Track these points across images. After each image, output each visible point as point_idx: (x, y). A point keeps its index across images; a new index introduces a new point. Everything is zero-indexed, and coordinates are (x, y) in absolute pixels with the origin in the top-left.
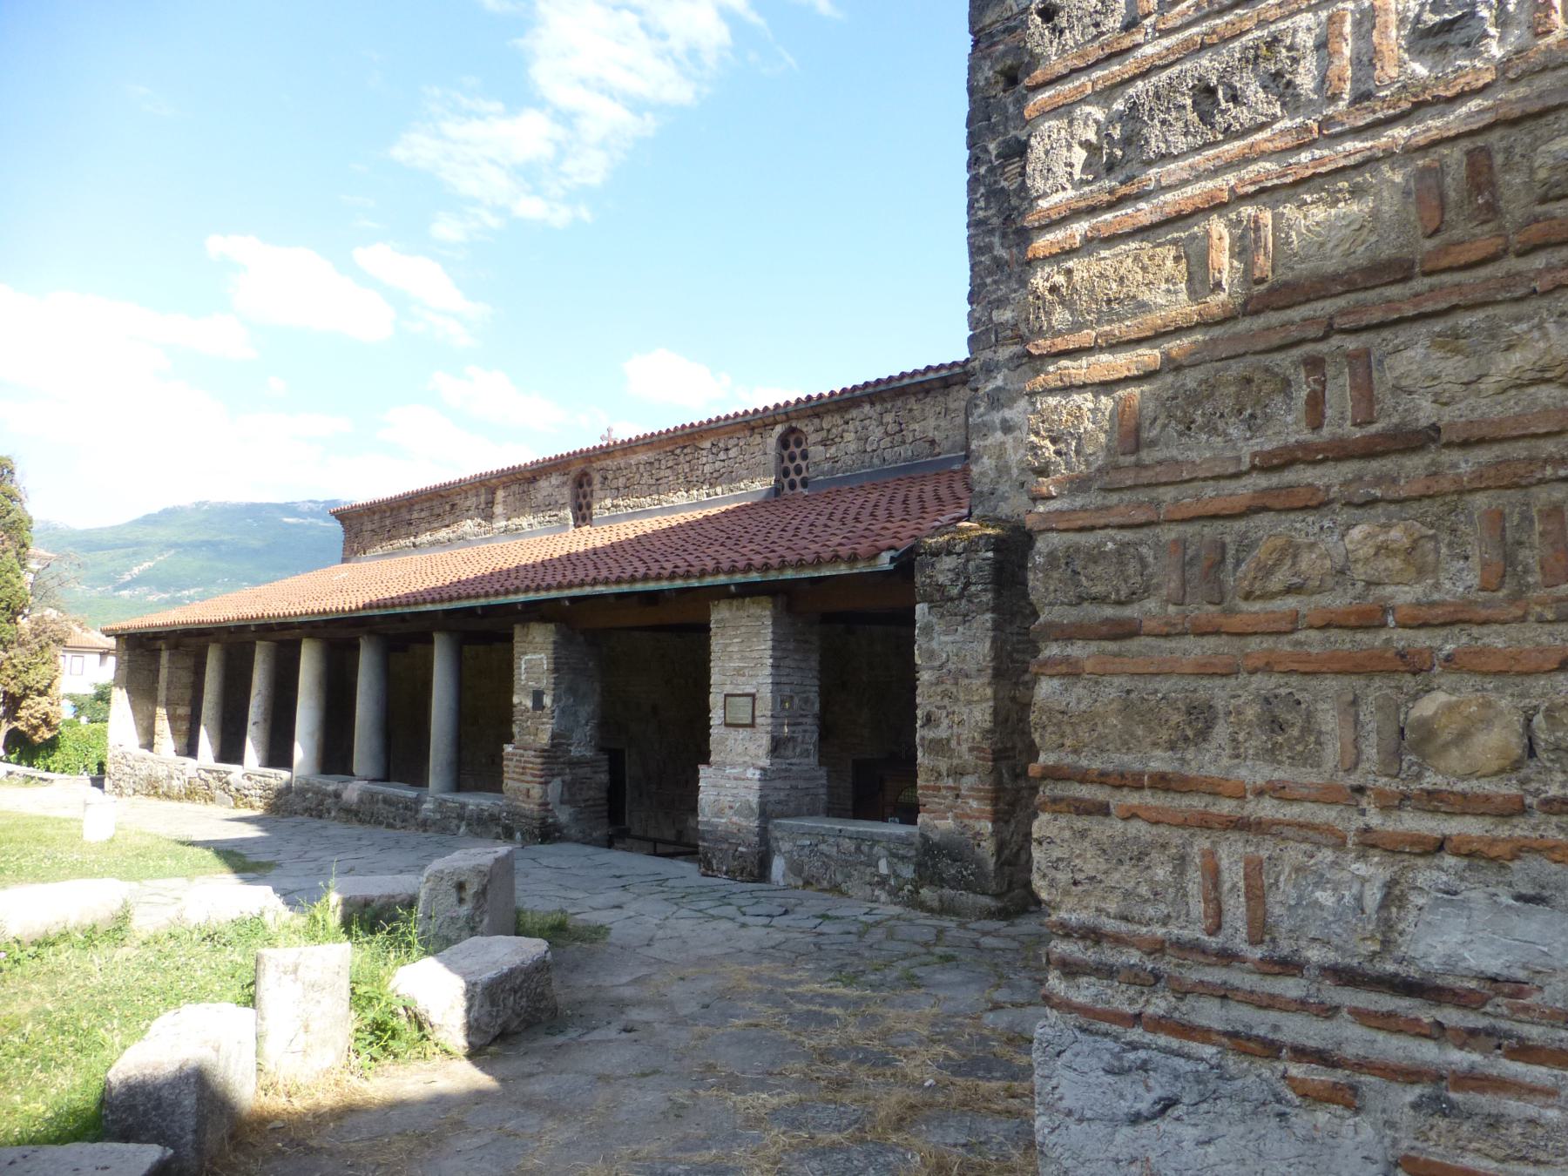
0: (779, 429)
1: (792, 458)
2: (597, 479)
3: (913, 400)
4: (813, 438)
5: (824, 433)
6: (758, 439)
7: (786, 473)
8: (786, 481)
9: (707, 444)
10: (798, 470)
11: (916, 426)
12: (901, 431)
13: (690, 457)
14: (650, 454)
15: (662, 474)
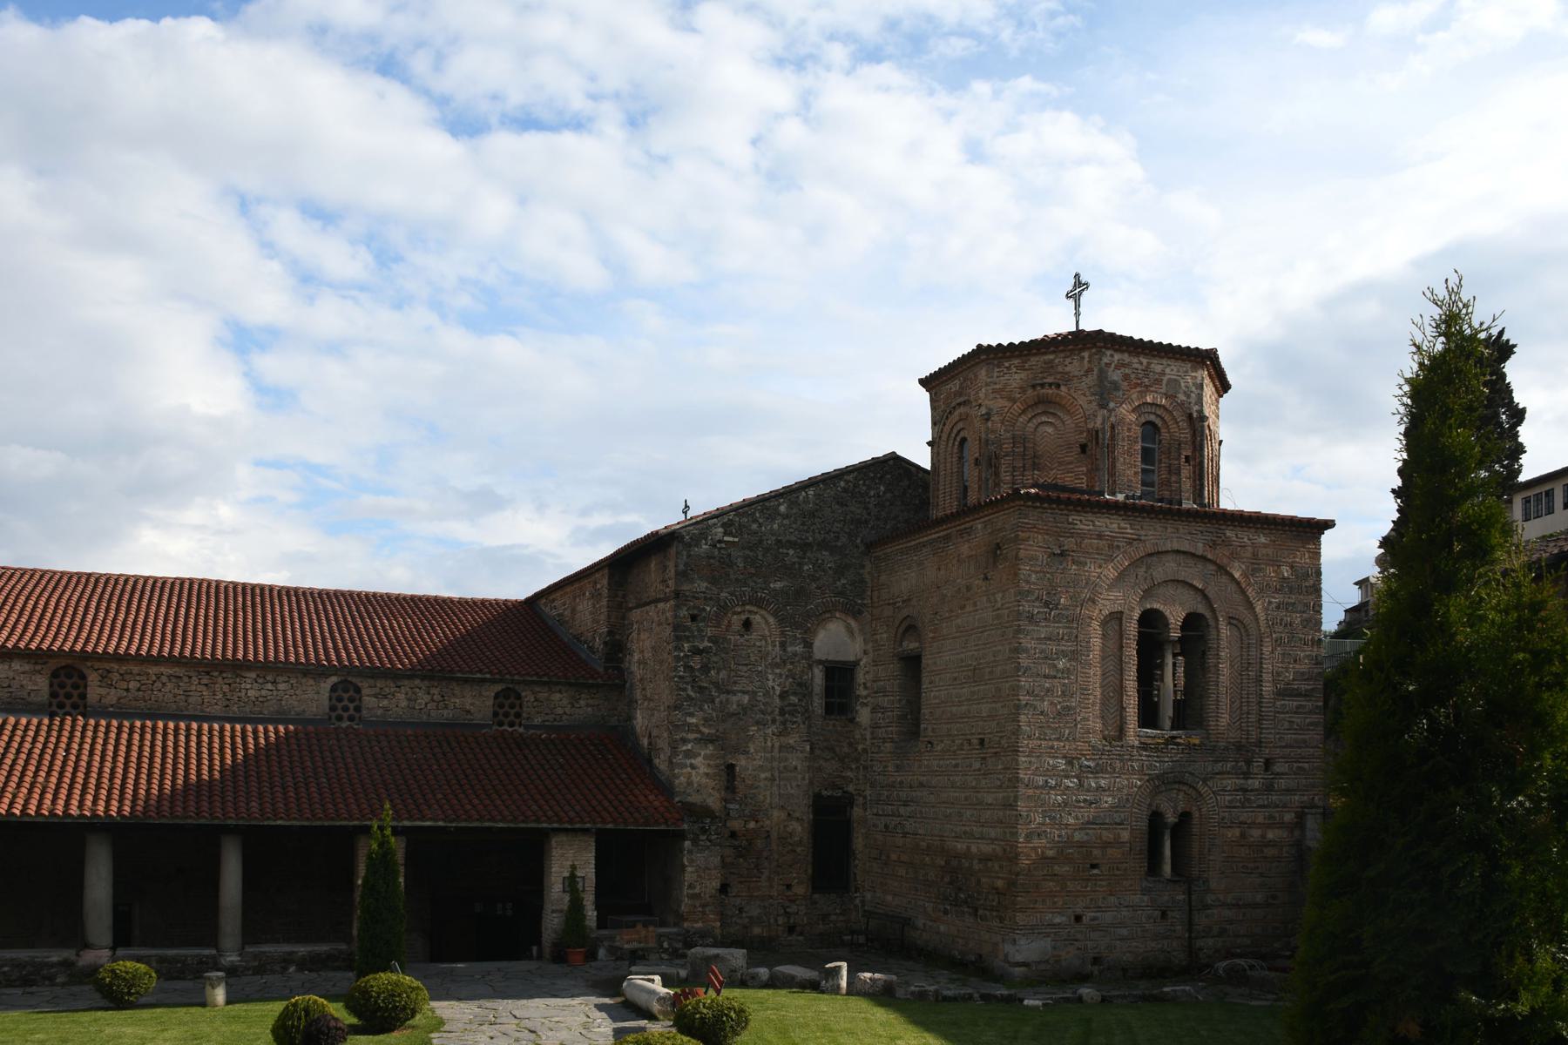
0: (334, 679)
1: (340, 700)
2: (93, 678)
3: (454, 684)
4: (364, 692)
5: (378, 690)
6: (312, 682)
7: (333, 709)
8: (334, 715)
9: (253, 675)
10: (346, 709)
11: (458, 701)
12: (444, 700)
13: (230, 681)
14: (177, 669)
15: (193, 688)
